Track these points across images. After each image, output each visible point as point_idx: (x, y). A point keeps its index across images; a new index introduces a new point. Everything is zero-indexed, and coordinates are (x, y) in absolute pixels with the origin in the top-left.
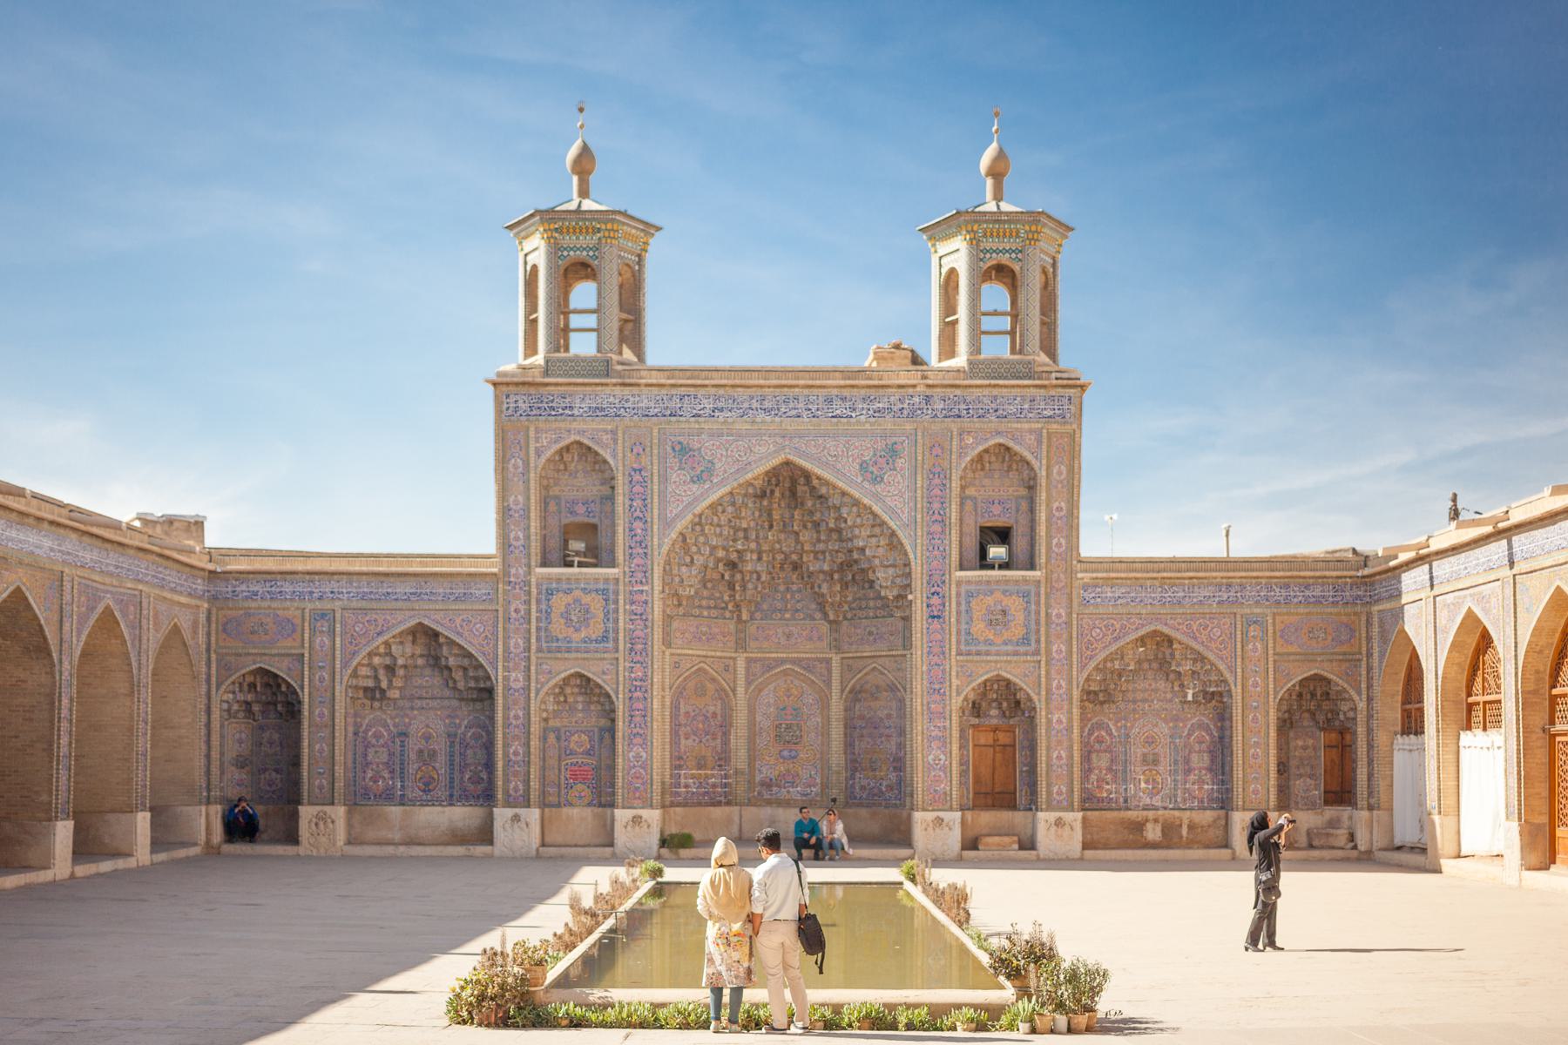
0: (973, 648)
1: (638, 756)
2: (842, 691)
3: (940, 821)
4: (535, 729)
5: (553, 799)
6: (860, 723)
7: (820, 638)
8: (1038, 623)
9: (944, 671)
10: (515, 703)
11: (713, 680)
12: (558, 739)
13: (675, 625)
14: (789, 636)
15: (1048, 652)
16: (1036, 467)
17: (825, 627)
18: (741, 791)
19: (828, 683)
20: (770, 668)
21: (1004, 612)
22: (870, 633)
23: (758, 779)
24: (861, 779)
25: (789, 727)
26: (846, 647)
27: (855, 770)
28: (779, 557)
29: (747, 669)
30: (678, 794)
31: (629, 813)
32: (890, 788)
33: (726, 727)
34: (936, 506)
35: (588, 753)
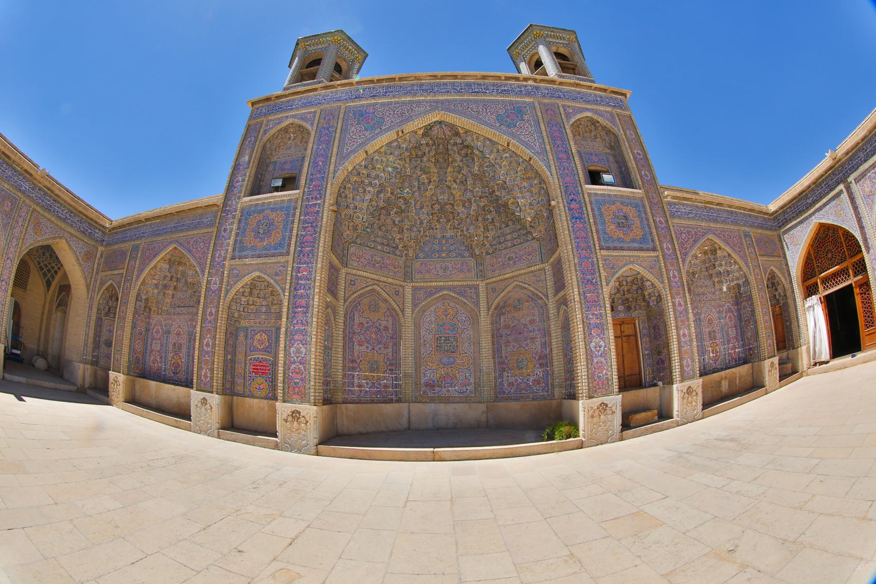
0: (611, 245)
1: (298, 351)
2: (489, 309)
3: (604, 405)
4: (221, 324)
5: (239, 389)
6: (504, 332)
7: (469, 270)
8: (649, 228)
9: (592, 264)
10: (212, 303)
11: (386, 301)
12: (246, 337)
13: (352, 250)
14: (445, 270)
15: (662, 248)
16: (615, 129)
17: (472, 262)
18: (409, 390)
19: (477, 304)
20: (432, 294)
21: (626, 218)
22: (509, 259)
23: (423, 381)
24: (508, 377)
25: (447, 339)
26: (490, 274)
27: (503, 370)
28: (437, 207)
29: (413, 295)
30: (352, 392)
31: (289, 407)
32: (537, 382)
33: (396, 339)
34: (559, 142)
35: (265, 350)
